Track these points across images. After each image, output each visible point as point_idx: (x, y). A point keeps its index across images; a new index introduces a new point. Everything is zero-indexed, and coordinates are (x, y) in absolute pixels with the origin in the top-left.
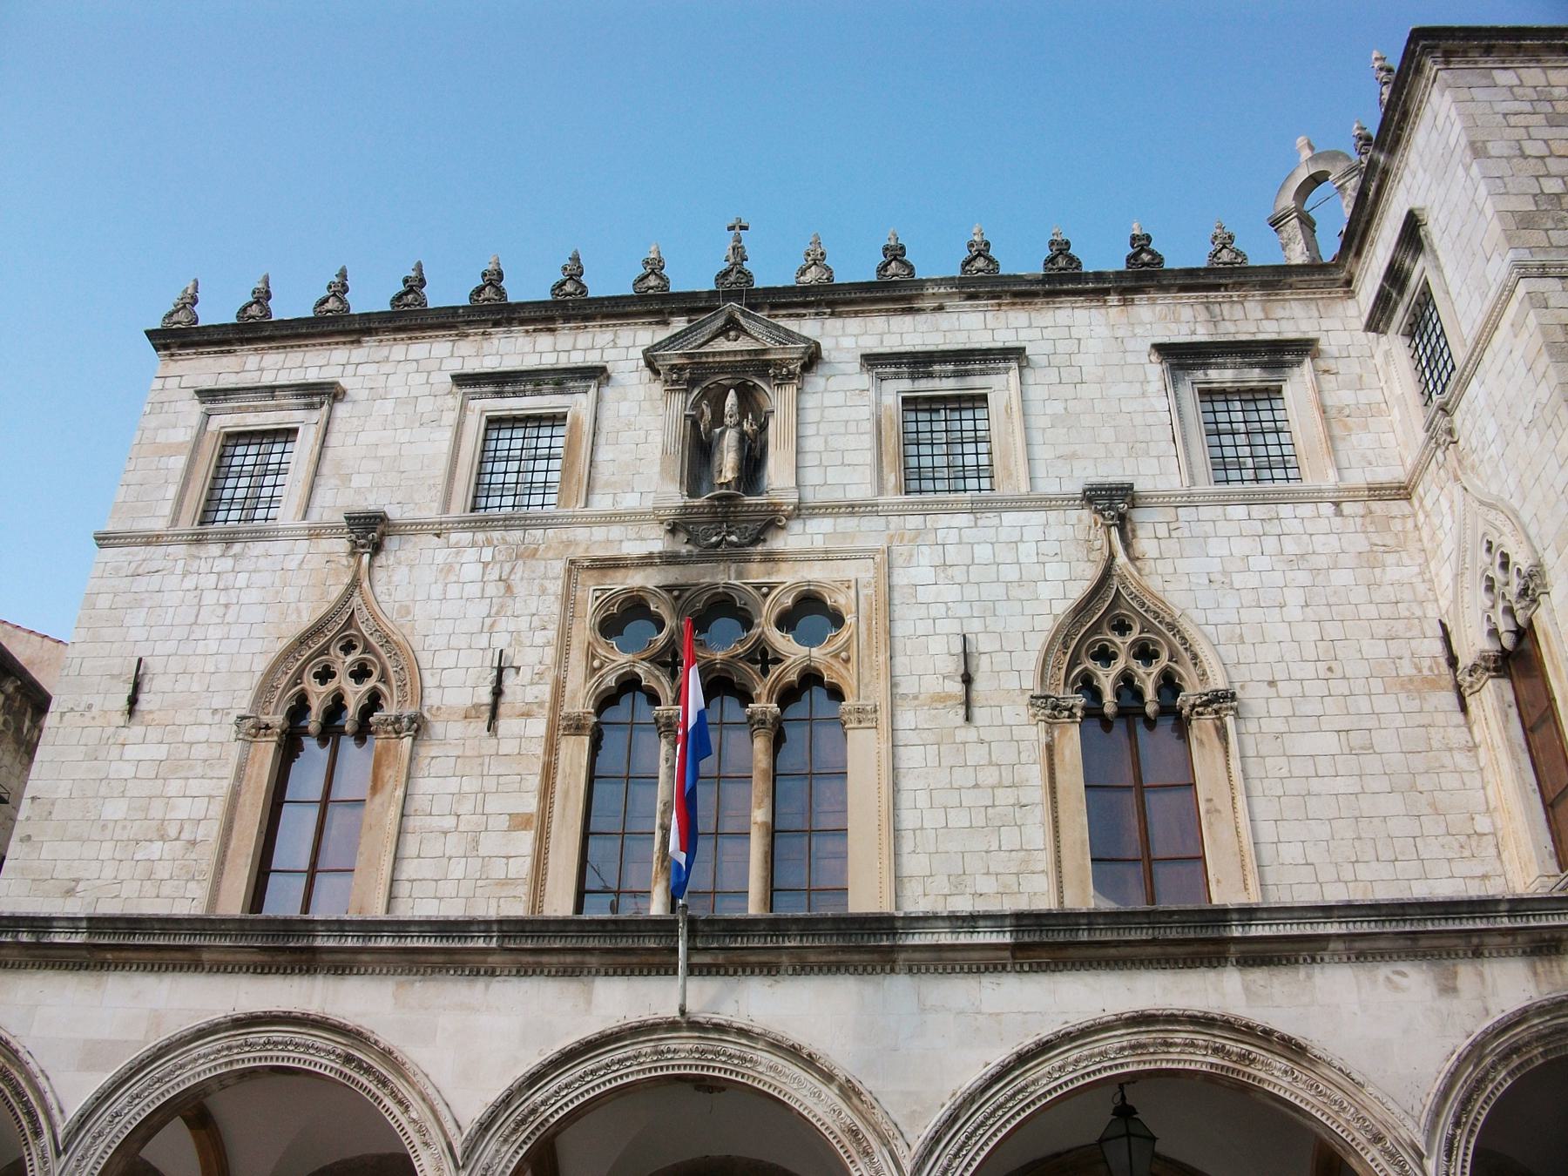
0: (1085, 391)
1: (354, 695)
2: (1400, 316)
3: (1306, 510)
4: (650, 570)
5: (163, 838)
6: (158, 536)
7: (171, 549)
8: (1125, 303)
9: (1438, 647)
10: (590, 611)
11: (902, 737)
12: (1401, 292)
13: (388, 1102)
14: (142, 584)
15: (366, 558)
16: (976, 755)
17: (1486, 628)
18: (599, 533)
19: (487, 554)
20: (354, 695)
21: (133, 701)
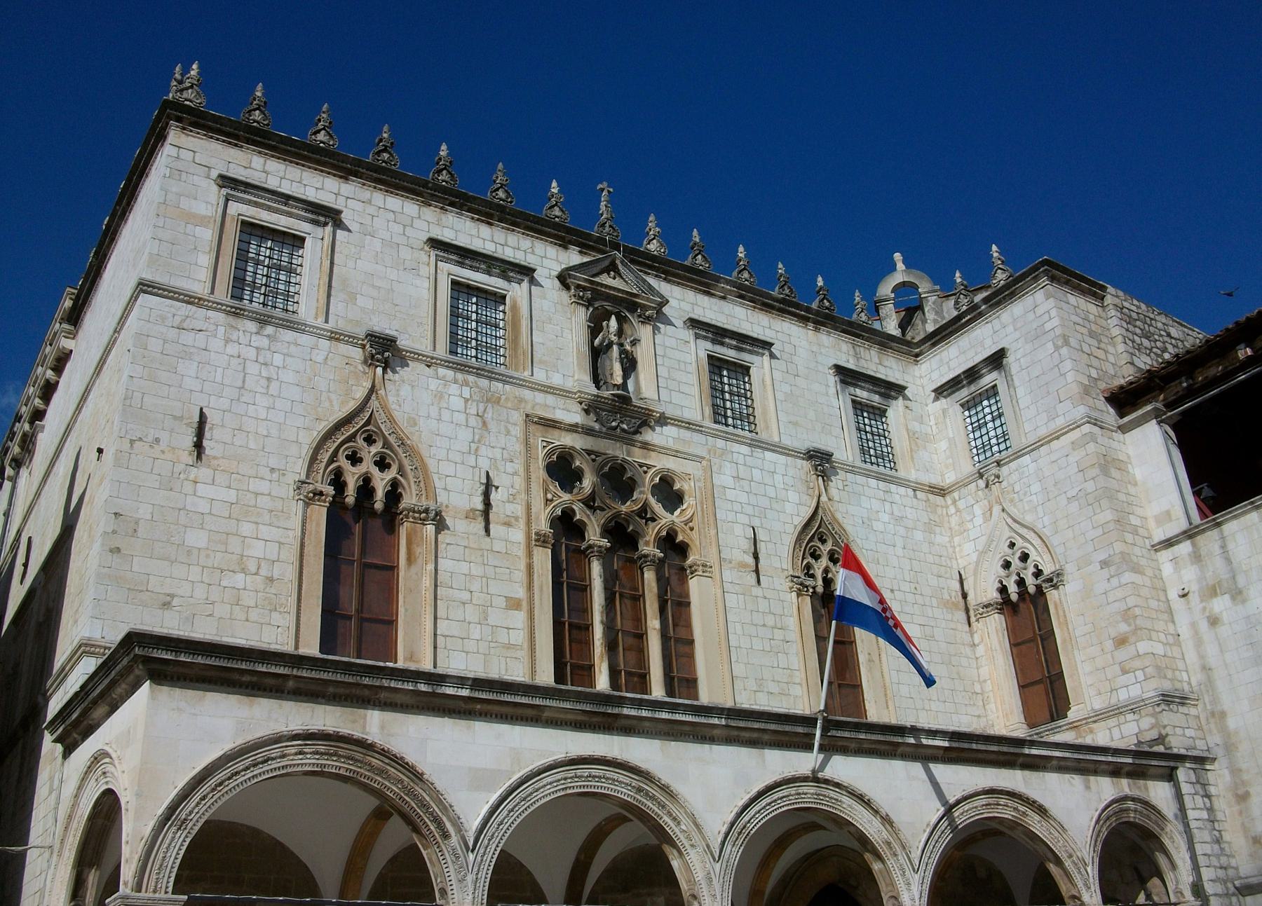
0: (801, 382)
1: (381, 483)
2: (964, 393)
3: (902, 490)
4: (575, 435)
5: (243, 571)
6: (200, 299)
7: (210, 313)
8: (816, 330)
9: (958, 586)
10: (541, 456)
11: (727, 586)
12: (970, 383)
13: (666, 818)
14: (188, 338)
15: (379, 370)
16: (763, 605)
17: (998, 585)
18: (540, 397)
19: (466, 392)
20: (381, 483)
21: (199, 446)
